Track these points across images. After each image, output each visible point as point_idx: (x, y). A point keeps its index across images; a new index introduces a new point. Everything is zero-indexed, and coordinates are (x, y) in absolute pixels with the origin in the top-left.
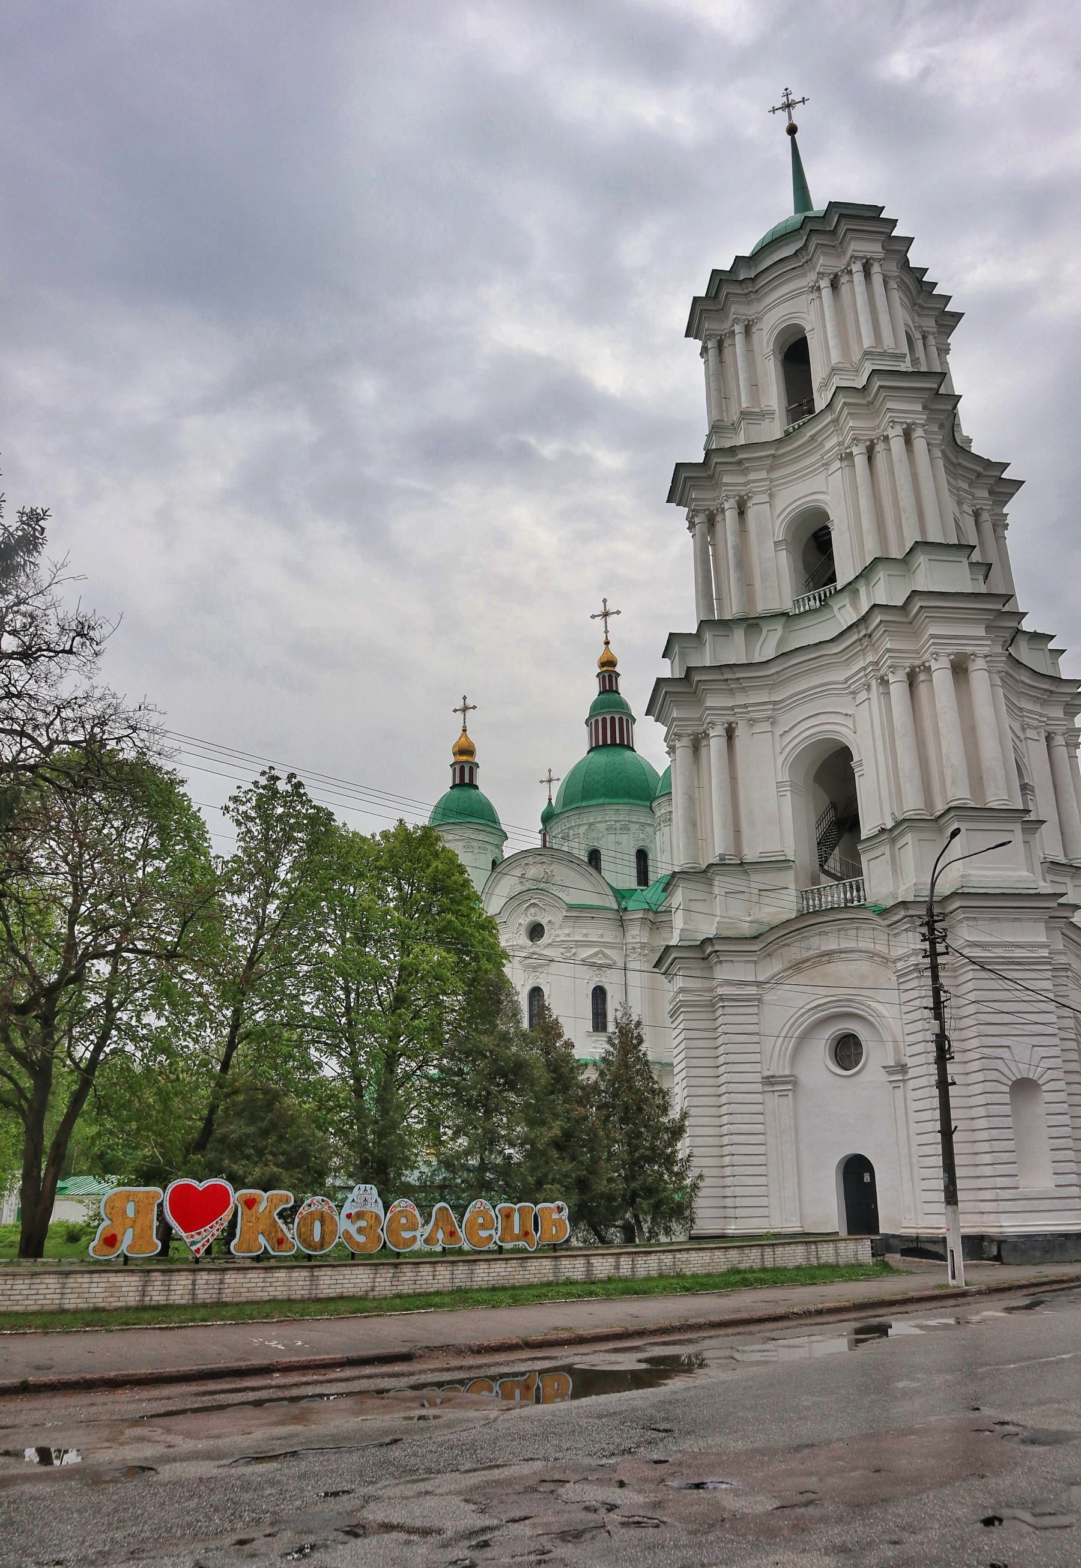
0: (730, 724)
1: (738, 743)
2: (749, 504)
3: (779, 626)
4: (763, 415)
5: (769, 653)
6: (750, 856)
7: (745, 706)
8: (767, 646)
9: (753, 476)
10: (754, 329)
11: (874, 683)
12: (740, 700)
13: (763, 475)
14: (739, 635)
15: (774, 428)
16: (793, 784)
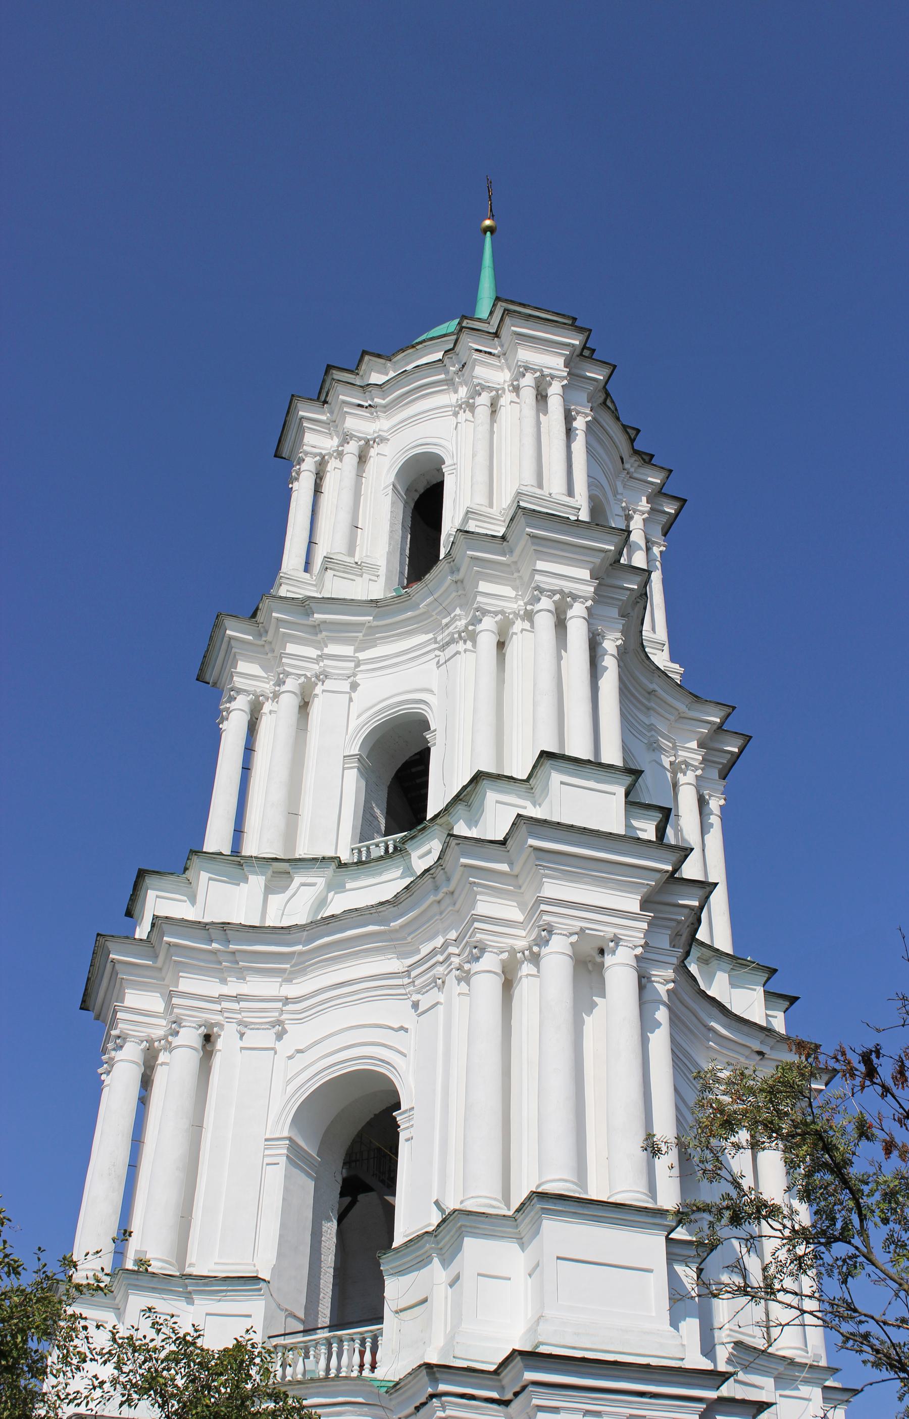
0: (210, 1025)
1: (218, 1061)
2: (318, 690)
3: (319, 880)
4: (359, 568)
5: (298, 915)
6: (199, 1265)
7: (237, 998)
8: (295, 904)
9: (332, 649)
10: (372, 452)
11: (451, 980)
12: (233, 987)
13: (348, 650)
14: (257, 882)
15: (375, 587)
16: (293, 1146)
